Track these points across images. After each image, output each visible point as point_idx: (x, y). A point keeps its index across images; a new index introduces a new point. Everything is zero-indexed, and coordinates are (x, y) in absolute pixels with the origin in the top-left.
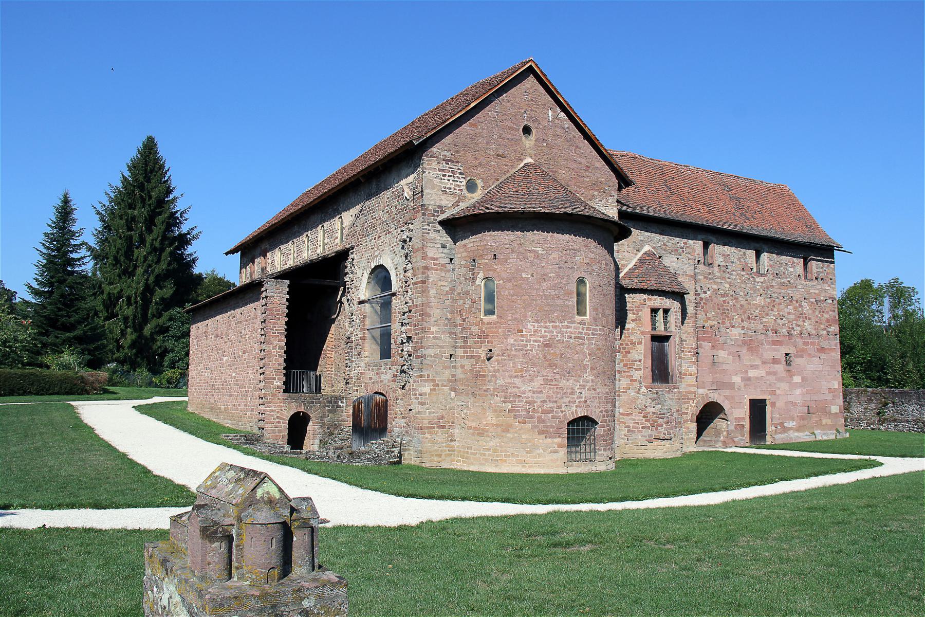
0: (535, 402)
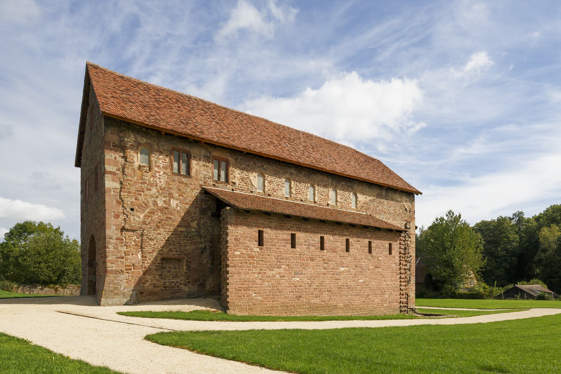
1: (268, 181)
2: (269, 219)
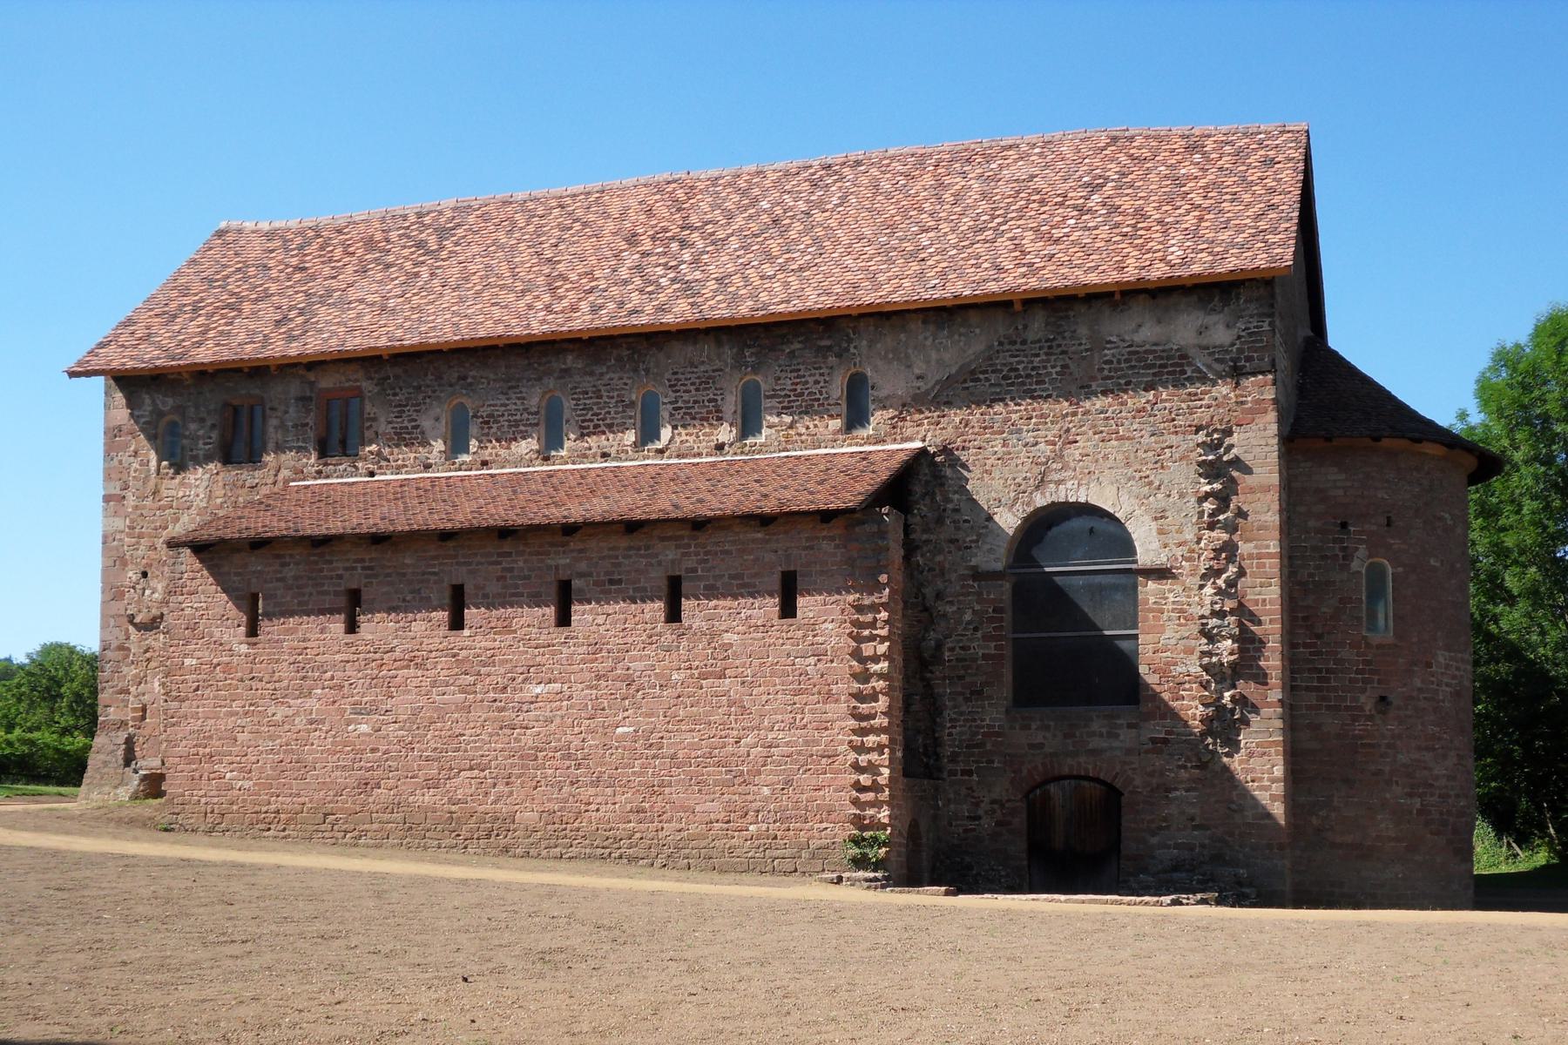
0: (1449, 796)
1: (481, 420)
2: (278, 556)
